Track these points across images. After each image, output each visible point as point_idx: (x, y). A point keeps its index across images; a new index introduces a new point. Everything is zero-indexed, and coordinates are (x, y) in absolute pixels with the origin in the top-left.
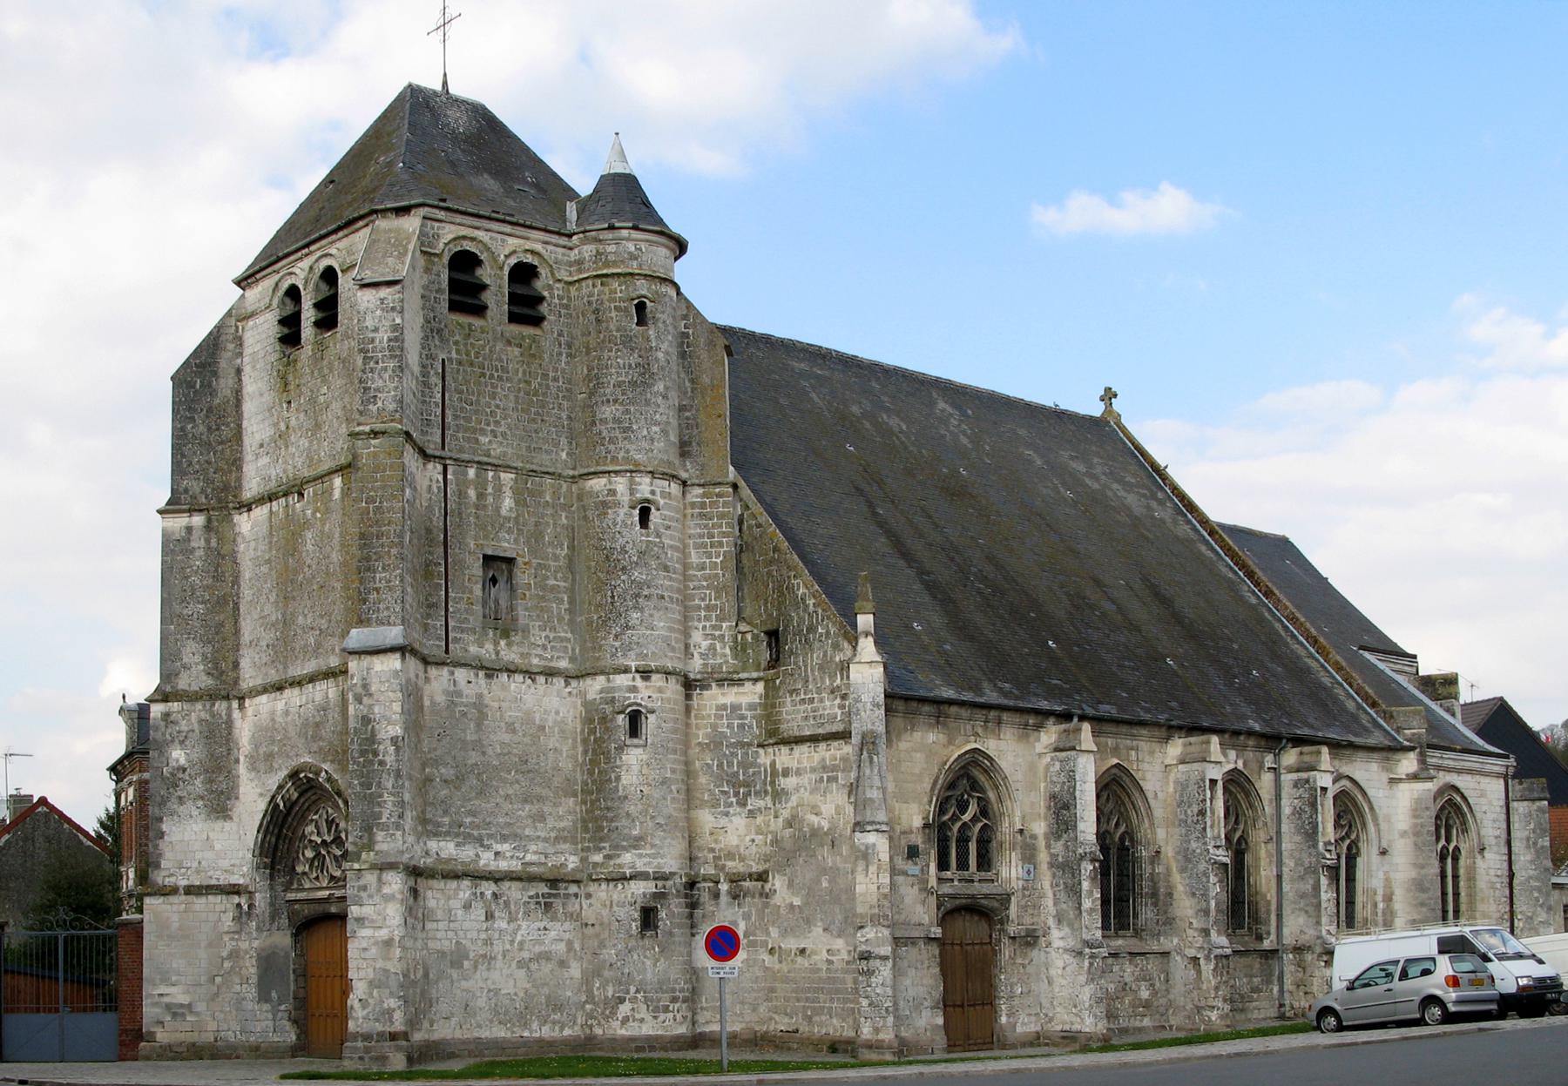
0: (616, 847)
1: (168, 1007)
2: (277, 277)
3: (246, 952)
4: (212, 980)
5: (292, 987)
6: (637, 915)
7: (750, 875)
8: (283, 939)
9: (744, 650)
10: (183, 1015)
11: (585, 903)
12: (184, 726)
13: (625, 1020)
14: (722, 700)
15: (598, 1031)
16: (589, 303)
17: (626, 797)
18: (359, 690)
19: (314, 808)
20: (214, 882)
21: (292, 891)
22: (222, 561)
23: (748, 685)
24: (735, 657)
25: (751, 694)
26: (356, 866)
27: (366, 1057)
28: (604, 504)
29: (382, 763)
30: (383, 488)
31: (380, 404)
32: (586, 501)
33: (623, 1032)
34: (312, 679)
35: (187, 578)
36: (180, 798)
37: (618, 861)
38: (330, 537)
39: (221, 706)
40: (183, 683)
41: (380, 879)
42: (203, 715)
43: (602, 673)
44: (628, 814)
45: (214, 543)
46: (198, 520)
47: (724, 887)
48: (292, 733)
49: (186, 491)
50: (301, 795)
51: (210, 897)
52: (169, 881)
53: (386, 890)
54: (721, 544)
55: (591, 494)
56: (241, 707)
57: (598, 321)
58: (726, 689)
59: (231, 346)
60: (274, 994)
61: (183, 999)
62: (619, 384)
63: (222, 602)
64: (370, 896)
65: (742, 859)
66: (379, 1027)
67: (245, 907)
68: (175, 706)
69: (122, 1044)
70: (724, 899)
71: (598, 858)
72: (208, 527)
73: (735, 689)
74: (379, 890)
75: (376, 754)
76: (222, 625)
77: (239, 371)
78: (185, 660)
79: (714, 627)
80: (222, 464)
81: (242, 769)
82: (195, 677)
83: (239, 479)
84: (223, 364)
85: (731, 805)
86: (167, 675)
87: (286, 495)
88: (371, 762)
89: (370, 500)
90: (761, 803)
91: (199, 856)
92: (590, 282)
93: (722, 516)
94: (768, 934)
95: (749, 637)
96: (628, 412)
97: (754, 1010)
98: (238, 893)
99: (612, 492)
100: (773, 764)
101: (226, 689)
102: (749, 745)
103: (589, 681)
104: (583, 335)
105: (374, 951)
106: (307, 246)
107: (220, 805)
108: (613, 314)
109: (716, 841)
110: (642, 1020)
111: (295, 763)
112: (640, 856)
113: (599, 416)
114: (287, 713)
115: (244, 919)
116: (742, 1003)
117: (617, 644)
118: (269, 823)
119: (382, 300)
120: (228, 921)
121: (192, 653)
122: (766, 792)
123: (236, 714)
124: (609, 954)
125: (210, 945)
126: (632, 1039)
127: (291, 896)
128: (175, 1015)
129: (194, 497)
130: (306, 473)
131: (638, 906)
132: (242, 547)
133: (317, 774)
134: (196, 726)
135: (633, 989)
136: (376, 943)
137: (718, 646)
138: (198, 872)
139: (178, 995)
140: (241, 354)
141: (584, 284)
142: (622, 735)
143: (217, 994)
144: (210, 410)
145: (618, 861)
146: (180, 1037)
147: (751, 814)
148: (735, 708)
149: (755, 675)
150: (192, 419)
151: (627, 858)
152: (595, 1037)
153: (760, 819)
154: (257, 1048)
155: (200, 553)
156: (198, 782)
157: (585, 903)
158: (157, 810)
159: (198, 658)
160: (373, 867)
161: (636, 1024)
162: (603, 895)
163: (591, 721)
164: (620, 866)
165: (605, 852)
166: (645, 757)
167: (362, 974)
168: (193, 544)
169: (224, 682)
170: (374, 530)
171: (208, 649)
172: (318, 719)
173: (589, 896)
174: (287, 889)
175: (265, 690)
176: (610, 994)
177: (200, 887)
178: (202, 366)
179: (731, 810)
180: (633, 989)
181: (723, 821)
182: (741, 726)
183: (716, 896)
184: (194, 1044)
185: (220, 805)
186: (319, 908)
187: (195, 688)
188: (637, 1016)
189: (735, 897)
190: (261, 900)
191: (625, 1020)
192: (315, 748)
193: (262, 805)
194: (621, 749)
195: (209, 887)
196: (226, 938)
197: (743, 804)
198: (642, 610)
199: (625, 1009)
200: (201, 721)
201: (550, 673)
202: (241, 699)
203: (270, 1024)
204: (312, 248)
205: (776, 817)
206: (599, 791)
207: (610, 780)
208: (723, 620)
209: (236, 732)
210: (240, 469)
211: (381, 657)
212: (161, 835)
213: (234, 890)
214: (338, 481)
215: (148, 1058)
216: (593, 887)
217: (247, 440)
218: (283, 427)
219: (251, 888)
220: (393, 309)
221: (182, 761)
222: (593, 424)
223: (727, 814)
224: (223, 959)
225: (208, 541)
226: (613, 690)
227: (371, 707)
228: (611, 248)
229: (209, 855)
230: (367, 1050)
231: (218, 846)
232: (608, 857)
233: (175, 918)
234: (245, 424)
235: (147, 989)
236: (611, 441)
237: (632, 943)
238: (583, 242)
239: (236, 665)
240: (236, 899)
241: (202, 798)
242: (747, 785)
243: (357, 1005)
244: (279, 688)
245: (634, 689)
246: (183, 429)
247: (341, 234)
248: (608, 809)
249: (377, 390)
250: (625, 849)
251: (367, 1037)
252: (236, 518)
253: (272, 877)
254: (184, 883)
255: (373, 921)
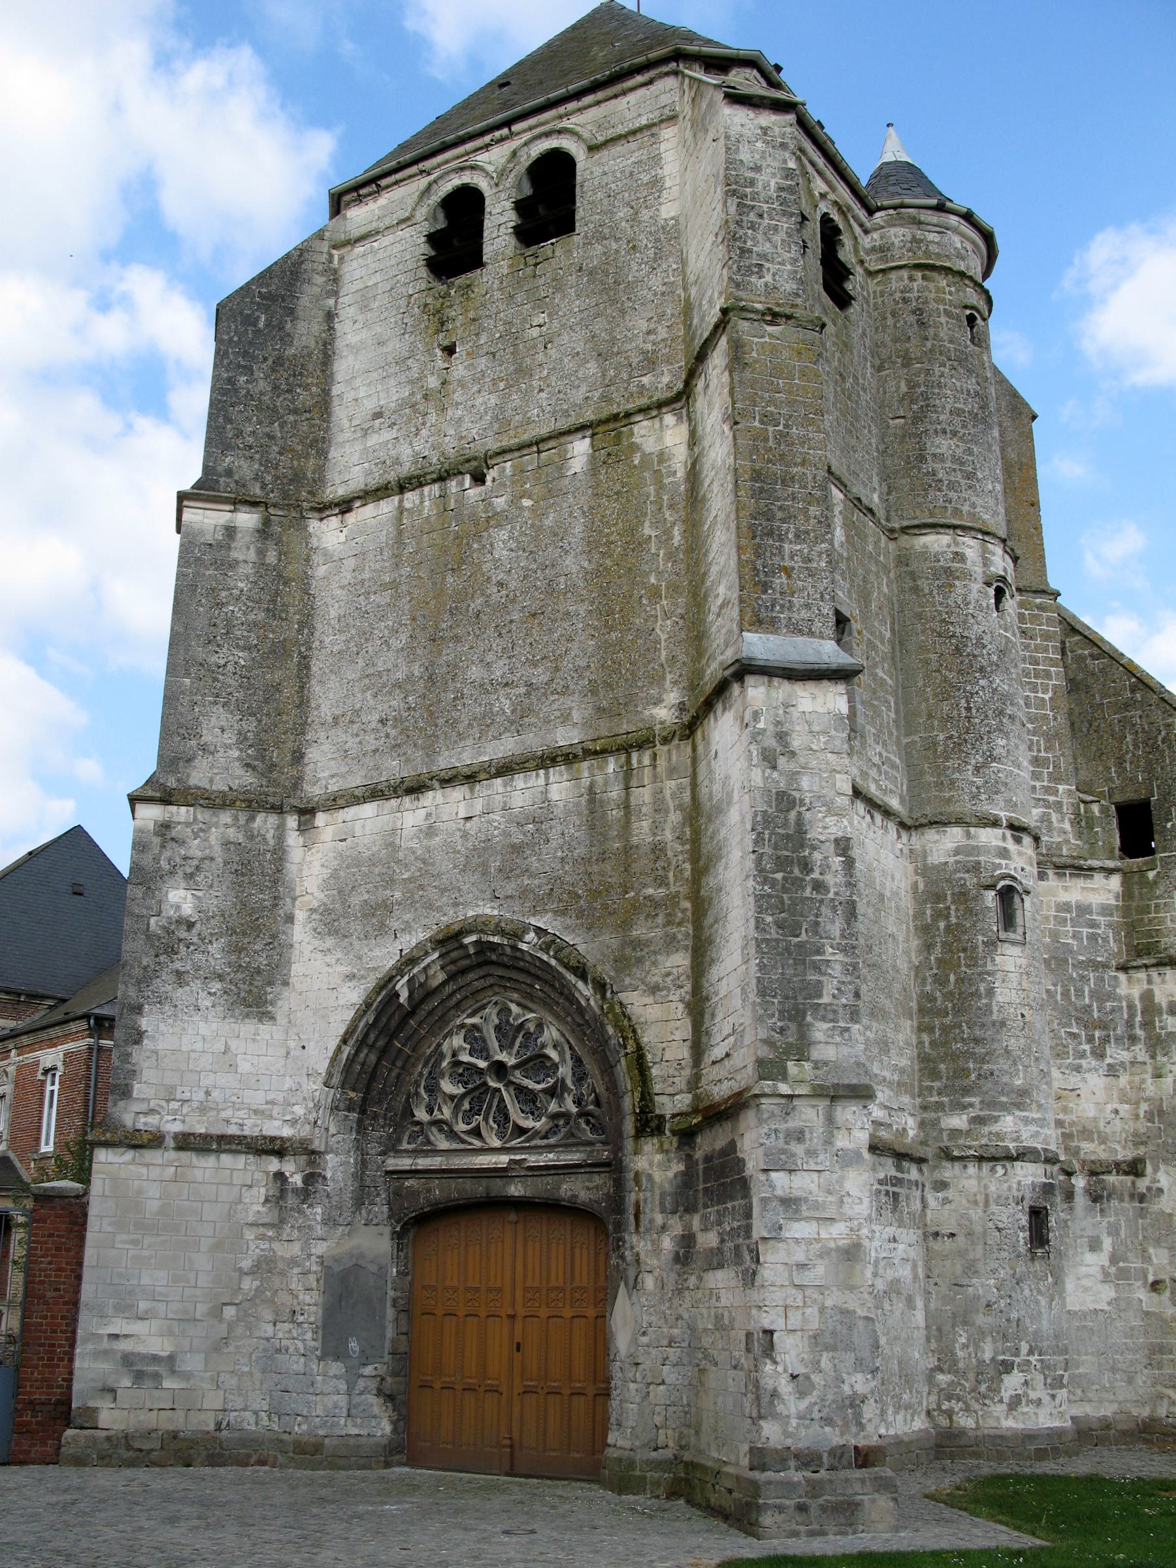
0: (992, 1104)
1: (128, 1360)
2: (424, 182)
3: (294, 1262)
4: (216, 1313)
5: (390, 1333)
6: (1024, 1220)
7: (1117, 1165)
8: (375, 1242)
9: (1090, 827)
10: (157, 1376)
11: (932, 1199)
12: (195, 848)
13: (1015, 1403)
14: (1064, 897)
15: (966, 1422)
16: (905, 301)
17: (1003, 1024)
18: (771, 742)
19: (471, 1004)
20: (232, 1130)
21: (399, 1153)
22: (284, 590)
23: (1098, 877)
24: (1079, 836)
25: (1103, 891)
26: (784, 1088)
27: (814, 1504)
28: (948, 571)
29: (818, 886)
30: (791, 403)
31: (768, 278)
32: (914, 566)
33: (1010, 1423)
34: (506, 769)
35: (220, 605)
36: (179, 974)
37: (995, 1128)
38: (559, 534)
39: (265, 823)
40: (199, 775)
41: (830, 1120)
42: (232, 833)
43: (959, 822)
44: (1007, 1051)
45: (271, 557)
46: (247, 519)
47: (1079, 1182)
48: (444, 864)
49: (229, 473)
50: (451, 977)
51: (226, 1159)
52: (143, 1122)
53: (842, 1142)
54: (1048, 675)
55: (924, 555)
56: (303, 829)
57: (922, 324)
58: (1068, 882)
59: (320, 280)
60: (353, 1345)
61: (158, 1346)
62: (958, 412)
63: (279, 651)
64: (812, 1153)
65: (1103, 1140)
66: (834, 1437)
67: (297, 1180)
68: (182, 813)
69: (21, 1429)
70: (1080, 1200)
71: (958, 1121)
72: (264, 532)
73: (1081, 883)
74: (828, 1142)
75: (806, 867)
76: (277, 688)
77: (330, 316)
78: (207, 738)
79: (1047, 790)
80: (293, 443)
81: (300, 934)
82: (221, 767)
83: (321, 469)
84: (304, 301)
85: (1082, 1055)
86: (172, 757)
87: (441, 479)
88: (799, 883)
89: (766, 418)
90: (1125, 1056)
91: (207, 1081)
92: (905, 274)
93: (1047, 637)
94: (1147, 1259)
95: (1095, 808)
96: (970, 452)
97: (1130, 1381)
98: (280, 1153)
99: (959, 557)
100: (1147, 997)
101: (280, 793)
102: (1105, 966)
103: (931, 835)
104: (896, 340)
105: (820, 1272)
106: (508, 123)
107: (253, 991)
108: (943, 319)
109: (1065, 1110)
110: (1039, 1402)
111: (450, 917)
112: (1026, 1121)
113: (931, 450)
114: (430, 831)
115: (291, 1201)
116: (1114, 1370)
117: (979, 781)
118: (370, 1027)
119: (765, 130)
120: (255, 1204)
121: (219, 727)
122: (1133, 1039)
123: (293, 839)
124: (984, 1286)
125: (217, 1247)
126: (1030, 1436)
127: (393, 1163)
128: (139, 1376)
129: (241, 484)
130: (493, 445)
131: (1027, 1204)
132: (321, 571)
133: (517, 935)
134: (218, 851)
135: (1024, 1348)
136: (824, 1253)
137: (1054, 817)
138: (203, 1109)
139: (149, 1338)
140: (336, 294)
141: (893, 275)
142: (992, 920)
143: (226, 1340)
144: (279, 361)
145: (995, 1128)
146: (150, 1420)
147: (1112, 1071)
148: (1083, 909)
149: (1110, 864)
150: (248, 370)
151: (1008, 1123)
152: (962, 1432)
153: (1124, 1080)
154: (317, 1448)
155: (246, 569)
156: (215, 948)
157: (932, 1199)
158: (132, 992)
159: (230, 738)
160: (819, 1092)
161: (1029, 1409)
162: (971, 1184)
163: (939, 897)
164: (999, 1136)
165: (973, 1113)
166: (1023, 961)
167: (795, 1320)
168: (235, 554)
169: (275, 783)
170: (777, 468)
171: (251, 725)
172: (517, 838)
173: (941, 1185)
174: (391, 1147)
175: (375, 794)
176: (987, 1356)
177: (206, 1137)
178: (270, 297)
179: (1083, 1062)
180: (1024, 1348)
181: (1074, 1080)
182: (1093, 938)
183: (1069, 1196)
184: (174, 1435)
185: (253, 991)
186: (478, 1189)
187: (220, 785)
188: (1033, 1395)
189: (1096, 1198)
190: (337, 1167)
191: (1015, 1403)
192: (510, 888)
193: (354, 995)
194: (992, 944)
195: (222, 1139)
196: (250, 1235)
197: (1100, 1055)
198: (1006, 735)
199: (1012, 1383)
200: (226, 844)
201: (887, 813)
202: (307, 813)
203: (342, 1400)
204: (515, 128)
205: (1158, 1076)
206: (957, 1011)
207: (976, 994)
208: (1058, 780)
209: (291, 868)
210: (323, 454)
211: (811, 686)
212: (138, 1037)
213: (275, 1148)
214: (580, 447)
215: (79, 1461)
216: (949, 1171)
217: (341, 414)
218: (433, 382)
219: (317, 1145)
220: (783, 146)
221: (187, 909)
222: (922, 458)
223: (1078, 1069)
224: (242, 1273)
225: (261, 553)
226: (976, 850)
227: (793, 776)
228: (931, 237)
229: (224, 1079)
230: (815, 1489)
231: (244, 1066)
232: (979, 1120)
233: (153, 1191)
234: (336, 390)
235: (87, 1323)
236: (952, 486)
237: (1021, 1268)
238: (891, 224)
239: (298, 757)
240: (274, 1164)
241: (221, 977)
242: (1104, 1026)
243: (785, 1387)
244: (415, 789)
245: (1004, 853)
246: (230, 381)
247: (588, 99)
248: (977, 1041)
249: (763, 256)
250: (1004, 1107)
251: (808, 1459)
252: (314, 525)
253: (361, 1128)
254: (177, 1127)
255: (816, 1206)
